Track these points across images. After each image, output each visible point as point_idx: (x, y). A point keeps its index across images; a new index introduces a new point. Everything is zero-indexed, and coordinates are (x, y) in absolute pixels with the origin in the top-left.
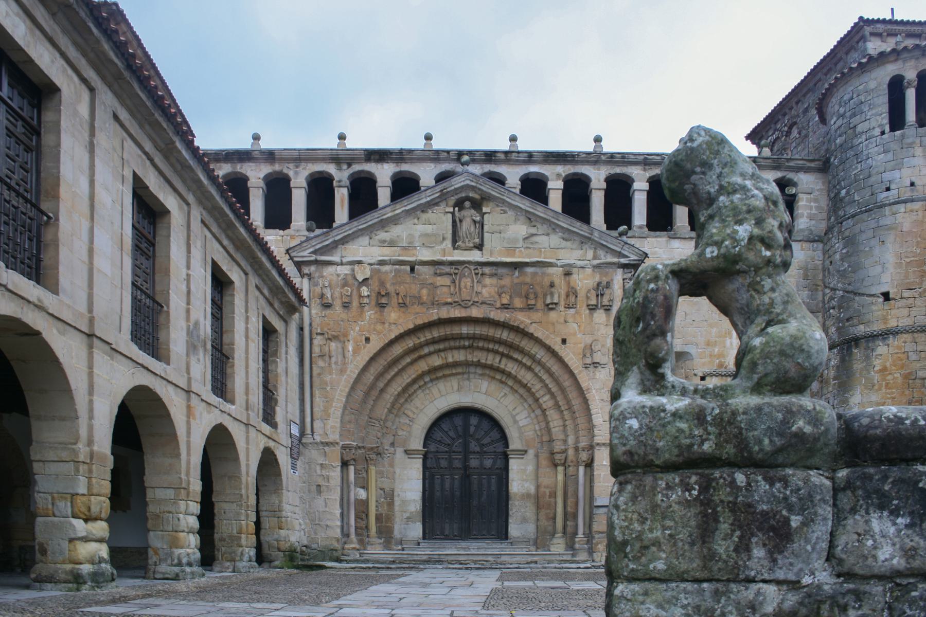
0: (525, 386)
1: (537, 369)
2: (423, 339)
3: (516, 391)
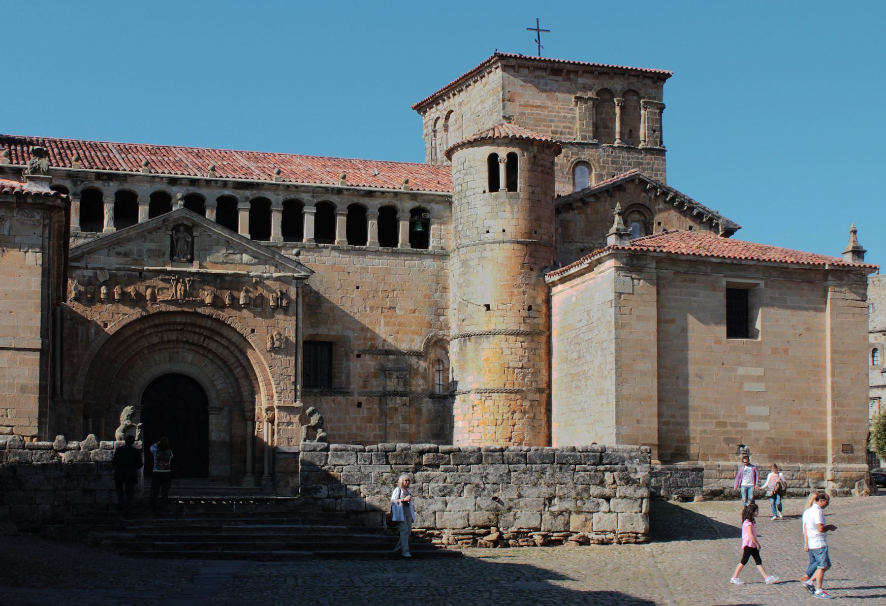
0: (222, 360)
1: (233, 348)
2: (147, 325)
3: (215, 363)
